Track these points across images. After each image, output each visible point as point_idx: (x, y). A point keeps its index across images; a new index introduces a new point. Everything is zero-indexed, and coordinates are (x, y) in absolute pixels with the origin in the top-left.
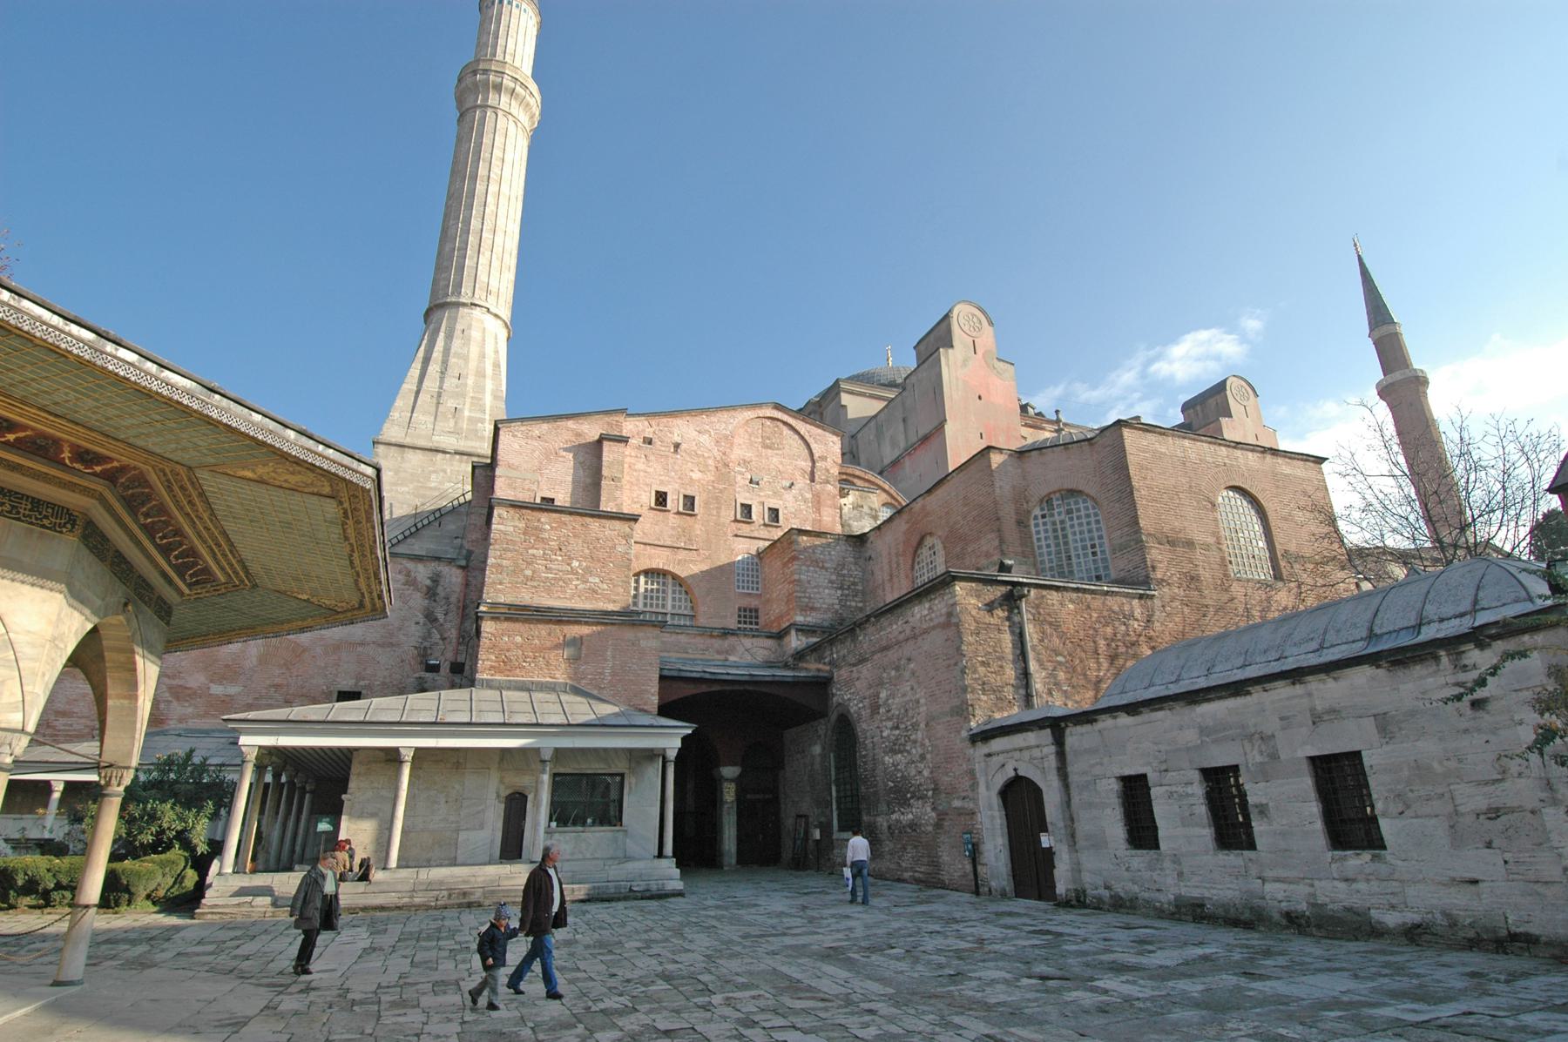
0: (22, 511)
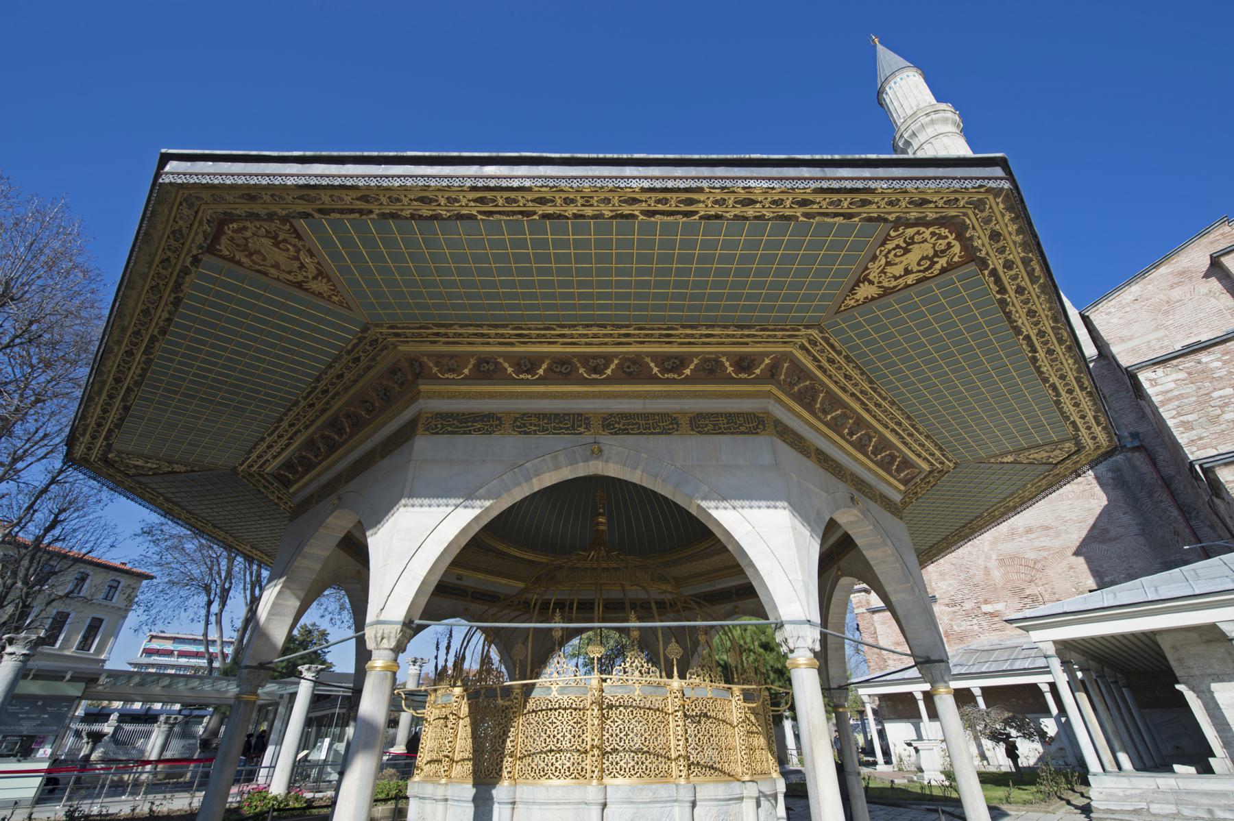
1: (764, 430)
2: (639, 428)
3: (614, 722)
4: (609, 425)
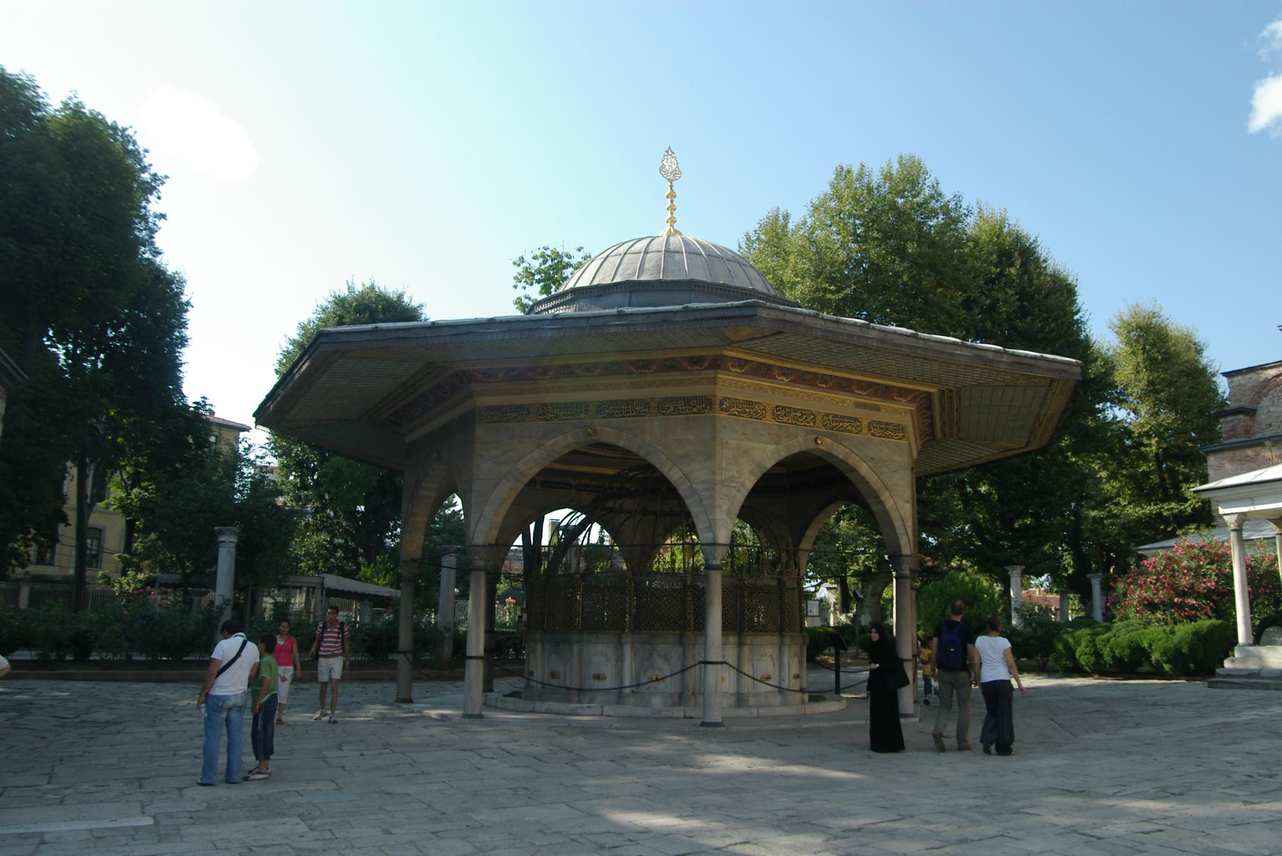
4: (601, 410)
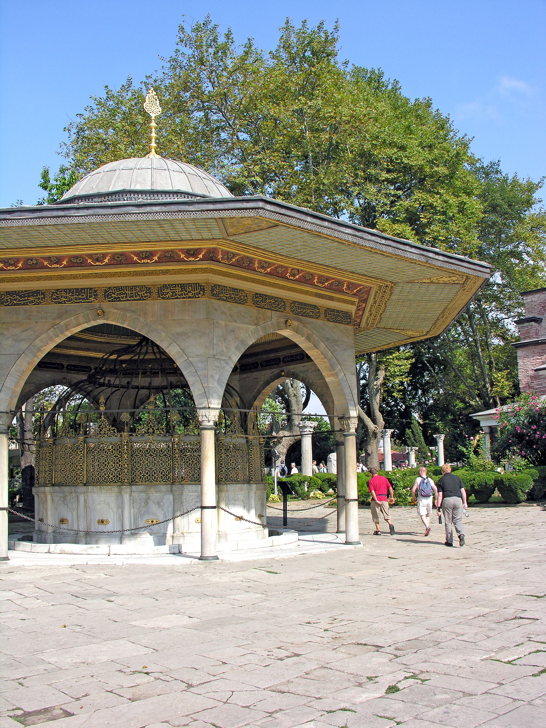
0: (177, 293)
1: (203, 295)
2: (126, 297)
3: (137, 455)
4: (108, 295)
